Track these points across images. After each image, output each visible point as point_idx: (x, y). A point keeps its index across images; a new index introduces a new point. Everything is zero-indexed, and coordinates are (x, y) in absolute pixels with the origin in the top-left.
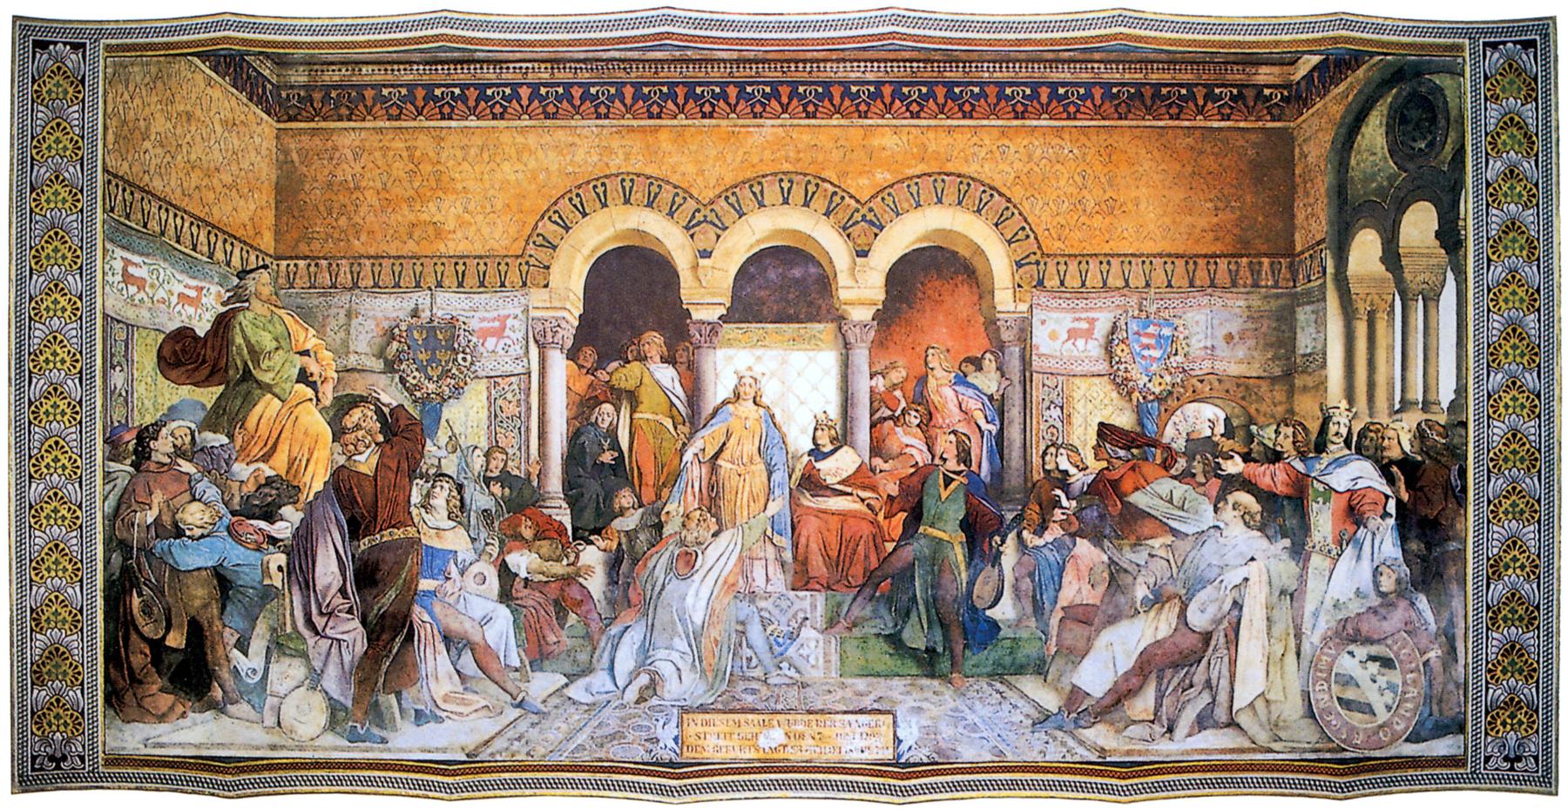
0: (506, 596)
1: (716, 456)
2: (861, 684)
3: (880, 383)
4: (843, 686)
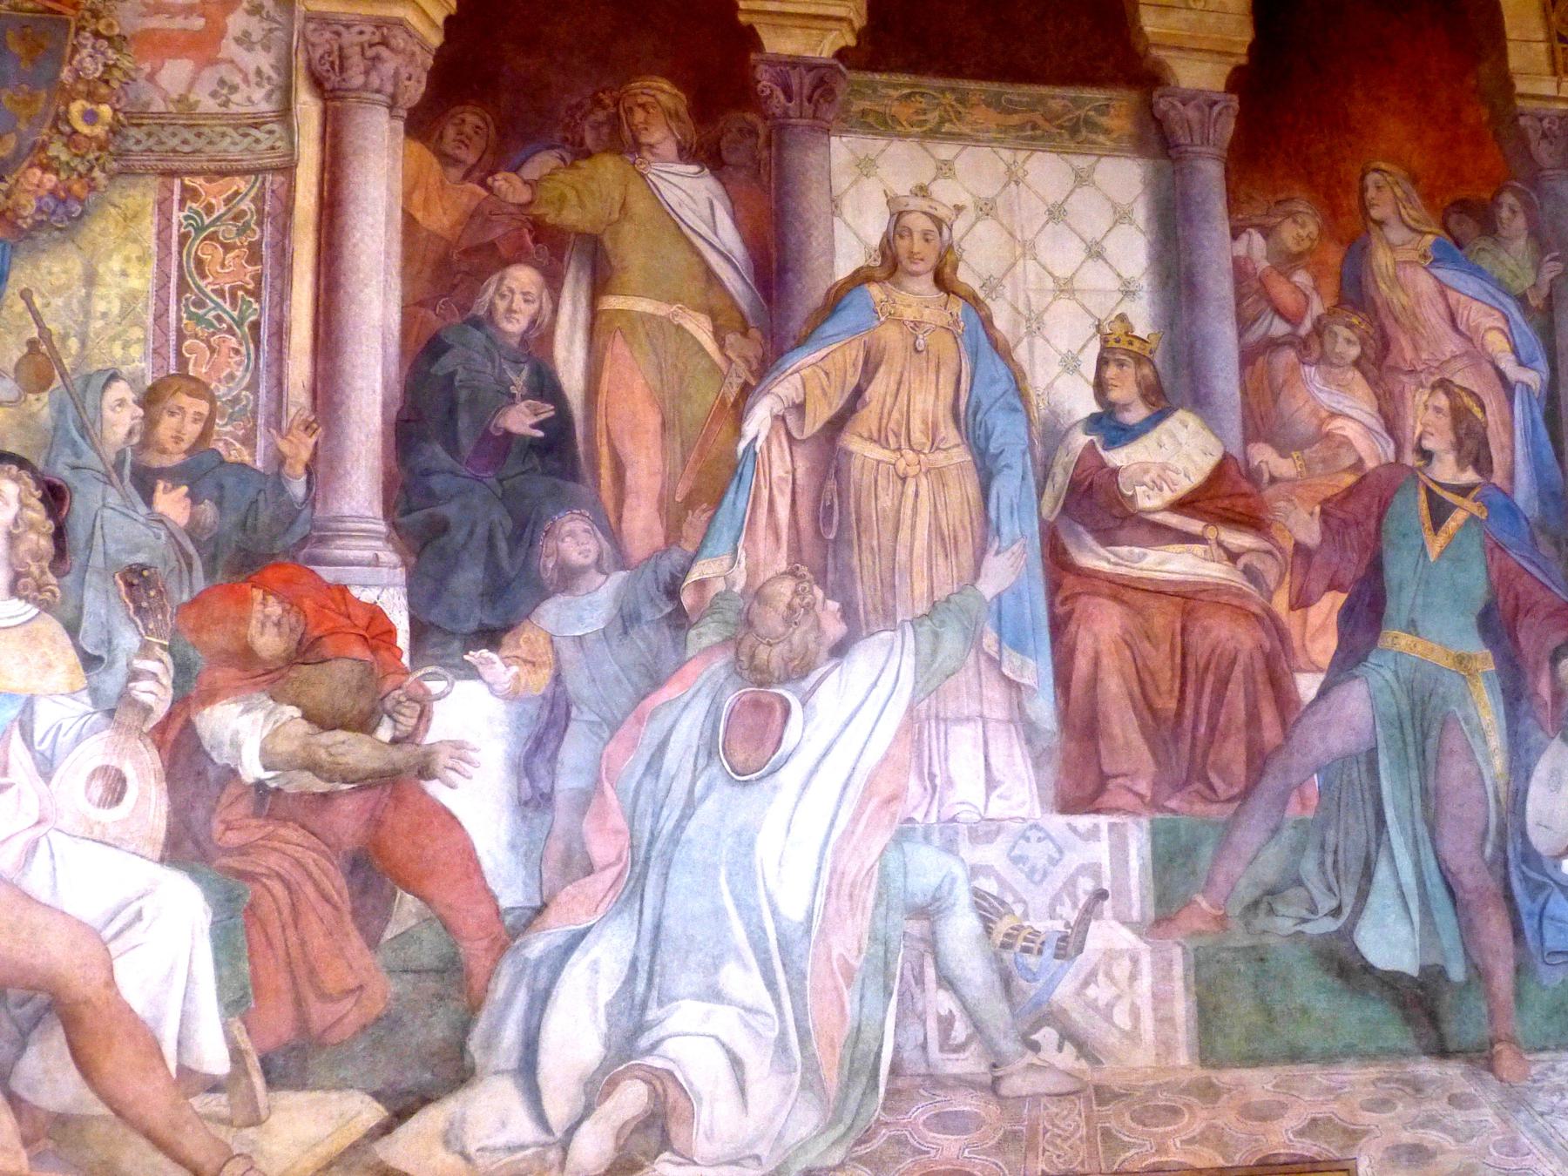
0: (183, 847)
1: (838, 424)
2: (1259, 1082)
3: (1255, 245)
4: (1209, 1092)
